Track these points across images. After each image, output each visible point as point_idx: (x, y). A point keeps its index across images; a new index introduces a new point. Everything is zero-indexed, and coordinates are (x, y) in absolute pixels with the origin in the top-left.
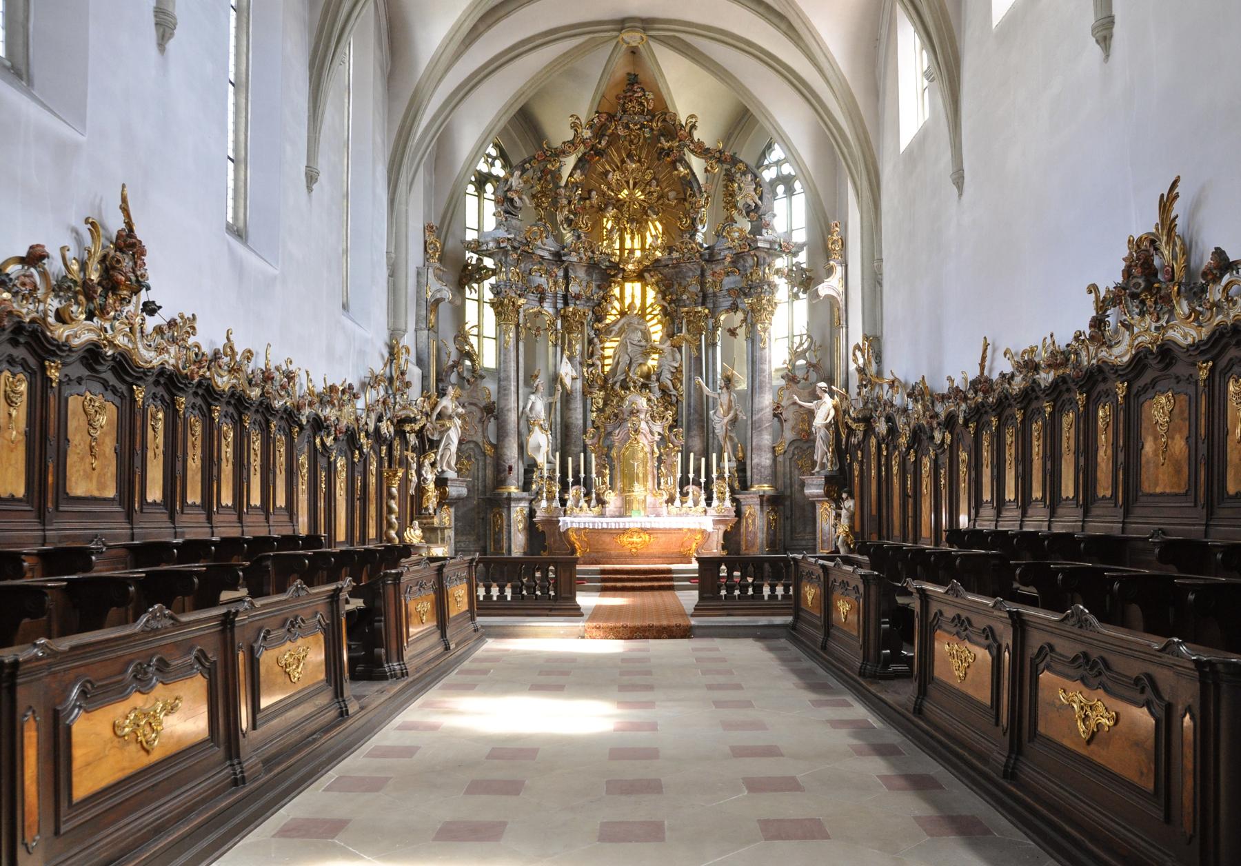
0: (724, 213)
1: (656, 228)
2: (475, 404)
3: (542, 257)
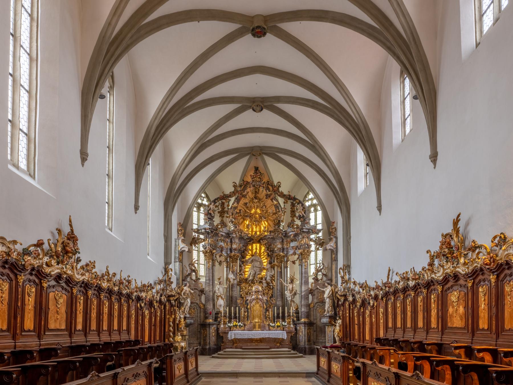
0: (291, 219)
1: (265, 224)
2: (197, 289)
3: (222, 235)
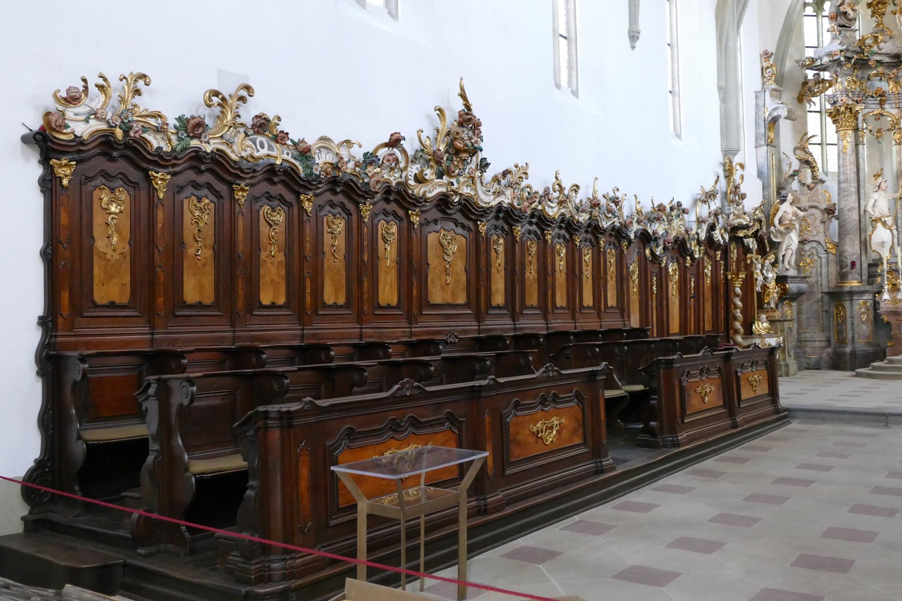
2: (815, 207)
3: (878, 61)
